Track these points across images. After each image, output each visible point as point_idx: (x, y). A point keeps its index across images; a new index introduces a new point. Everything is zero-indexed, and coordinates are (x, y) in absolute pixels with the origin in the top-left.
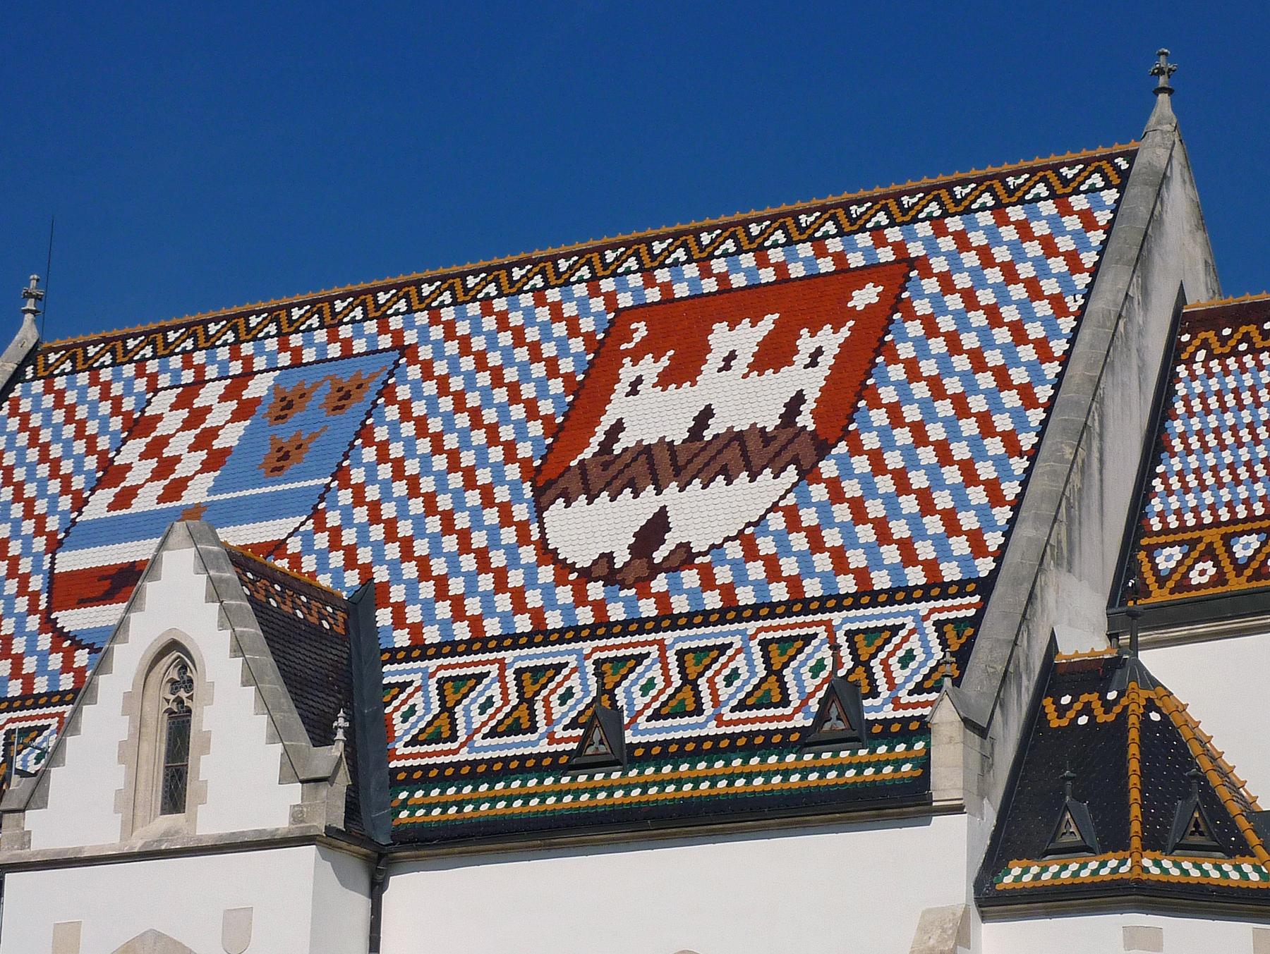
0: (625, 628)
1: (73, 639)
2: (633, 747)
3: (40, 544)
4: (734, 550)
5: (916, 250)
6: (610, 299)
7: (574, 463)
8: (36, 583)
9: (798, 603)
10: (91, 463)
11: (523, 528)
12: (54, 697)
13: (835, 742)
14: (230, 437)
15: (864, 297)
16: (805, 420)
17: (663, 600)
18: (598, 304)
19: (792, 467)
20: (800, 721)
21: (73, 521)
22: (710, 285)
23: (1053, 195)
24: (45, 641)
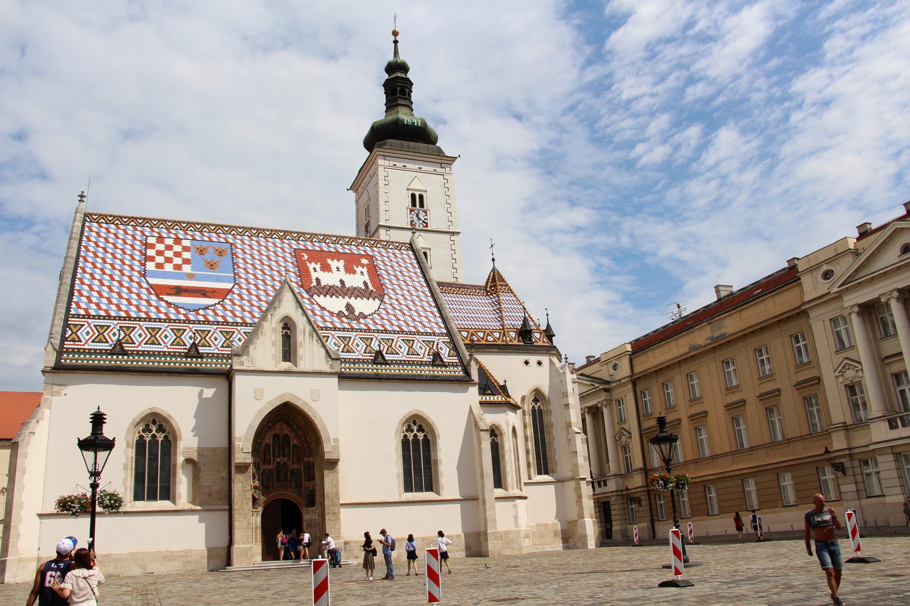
0: (361, 330)
1: (174, 304)
2: (388, 360)
3: (136, 274)
4: (375, 315)
5: (371, 254)
6: (289, 244)
7: (312, 286)
8: (145, 285)
9: (403, 332)
10: (137, 253)
11: (309, 299)
12: (180, 321)
13: (437, 366)
14: (186, 255)
15: (365, 261)
16: (371, 288)
17: (366, 325)
18: (286, 246)
19: (376, 299)
20: (425, 359)
21: (144, 269)
22: (318, 249)
23: (396, 249)
24: (163, 304)
